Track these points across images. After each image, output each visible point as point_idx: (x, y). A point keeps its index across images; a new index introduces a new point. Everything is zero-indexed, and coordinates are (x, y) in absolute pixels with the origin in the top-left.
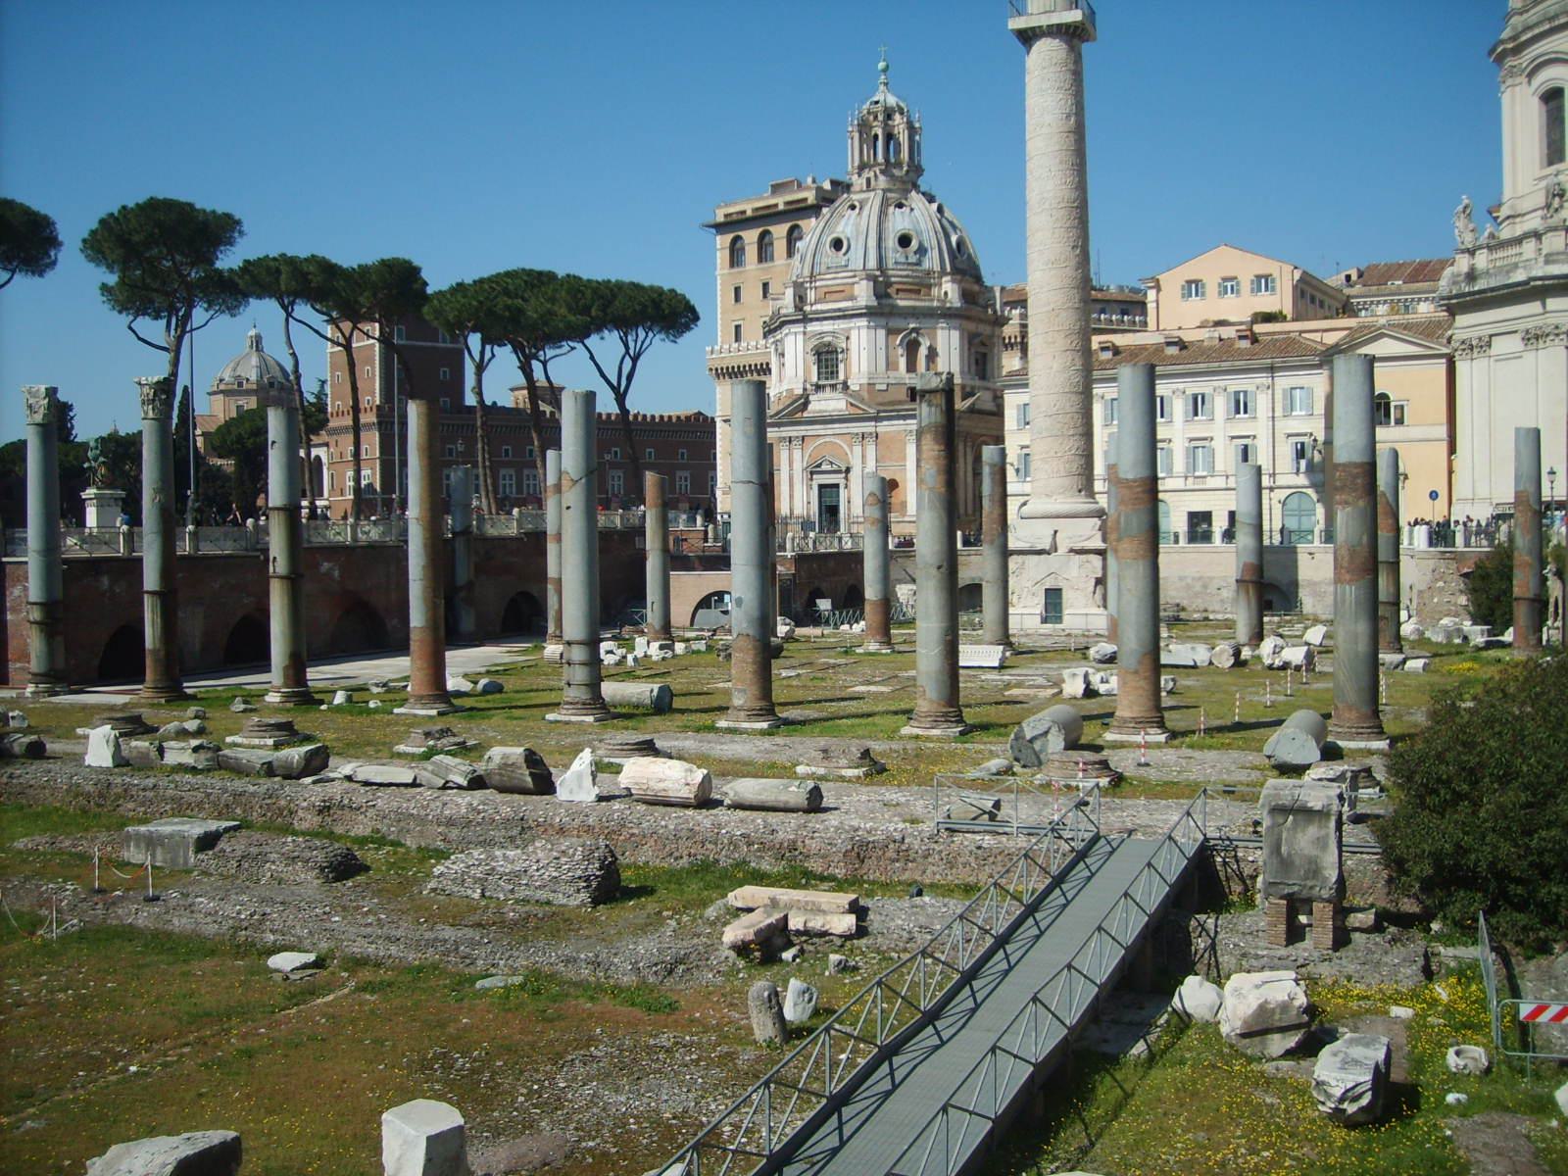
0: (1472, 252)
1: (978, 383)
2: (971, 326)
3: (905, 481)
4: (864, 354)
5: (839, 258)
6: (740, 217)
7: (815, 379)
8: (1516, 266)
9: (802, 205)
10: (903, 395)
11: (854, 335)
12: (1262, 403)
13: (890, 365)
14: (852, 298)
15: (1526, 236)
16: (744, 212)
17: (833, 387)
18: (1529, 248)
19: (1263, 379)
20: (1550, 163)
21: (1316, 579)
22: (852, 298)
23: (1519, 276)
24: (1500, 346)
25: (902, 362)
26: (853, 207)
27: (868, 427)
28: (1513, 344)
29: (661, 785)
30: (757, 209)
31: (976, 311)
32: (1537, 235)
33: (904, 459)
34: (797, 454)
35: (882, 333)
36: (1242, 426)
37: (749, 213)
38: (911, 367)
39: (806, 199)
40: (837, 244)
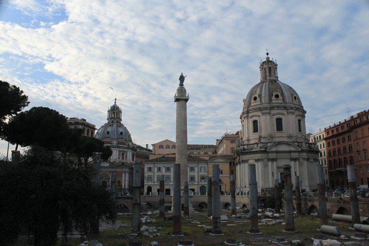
12: (196, 169)
13: (119, 158)
17: (107, 162)
18: (256, 146)
19: (196, 165)
20: (254, 132)
23: (254, 150)
27: (114, 170)
32: (257, 144)
33: (122, 177)
35: (117, 153)
36: (192, 174)
38: (123, 158)
40: (108, 133)
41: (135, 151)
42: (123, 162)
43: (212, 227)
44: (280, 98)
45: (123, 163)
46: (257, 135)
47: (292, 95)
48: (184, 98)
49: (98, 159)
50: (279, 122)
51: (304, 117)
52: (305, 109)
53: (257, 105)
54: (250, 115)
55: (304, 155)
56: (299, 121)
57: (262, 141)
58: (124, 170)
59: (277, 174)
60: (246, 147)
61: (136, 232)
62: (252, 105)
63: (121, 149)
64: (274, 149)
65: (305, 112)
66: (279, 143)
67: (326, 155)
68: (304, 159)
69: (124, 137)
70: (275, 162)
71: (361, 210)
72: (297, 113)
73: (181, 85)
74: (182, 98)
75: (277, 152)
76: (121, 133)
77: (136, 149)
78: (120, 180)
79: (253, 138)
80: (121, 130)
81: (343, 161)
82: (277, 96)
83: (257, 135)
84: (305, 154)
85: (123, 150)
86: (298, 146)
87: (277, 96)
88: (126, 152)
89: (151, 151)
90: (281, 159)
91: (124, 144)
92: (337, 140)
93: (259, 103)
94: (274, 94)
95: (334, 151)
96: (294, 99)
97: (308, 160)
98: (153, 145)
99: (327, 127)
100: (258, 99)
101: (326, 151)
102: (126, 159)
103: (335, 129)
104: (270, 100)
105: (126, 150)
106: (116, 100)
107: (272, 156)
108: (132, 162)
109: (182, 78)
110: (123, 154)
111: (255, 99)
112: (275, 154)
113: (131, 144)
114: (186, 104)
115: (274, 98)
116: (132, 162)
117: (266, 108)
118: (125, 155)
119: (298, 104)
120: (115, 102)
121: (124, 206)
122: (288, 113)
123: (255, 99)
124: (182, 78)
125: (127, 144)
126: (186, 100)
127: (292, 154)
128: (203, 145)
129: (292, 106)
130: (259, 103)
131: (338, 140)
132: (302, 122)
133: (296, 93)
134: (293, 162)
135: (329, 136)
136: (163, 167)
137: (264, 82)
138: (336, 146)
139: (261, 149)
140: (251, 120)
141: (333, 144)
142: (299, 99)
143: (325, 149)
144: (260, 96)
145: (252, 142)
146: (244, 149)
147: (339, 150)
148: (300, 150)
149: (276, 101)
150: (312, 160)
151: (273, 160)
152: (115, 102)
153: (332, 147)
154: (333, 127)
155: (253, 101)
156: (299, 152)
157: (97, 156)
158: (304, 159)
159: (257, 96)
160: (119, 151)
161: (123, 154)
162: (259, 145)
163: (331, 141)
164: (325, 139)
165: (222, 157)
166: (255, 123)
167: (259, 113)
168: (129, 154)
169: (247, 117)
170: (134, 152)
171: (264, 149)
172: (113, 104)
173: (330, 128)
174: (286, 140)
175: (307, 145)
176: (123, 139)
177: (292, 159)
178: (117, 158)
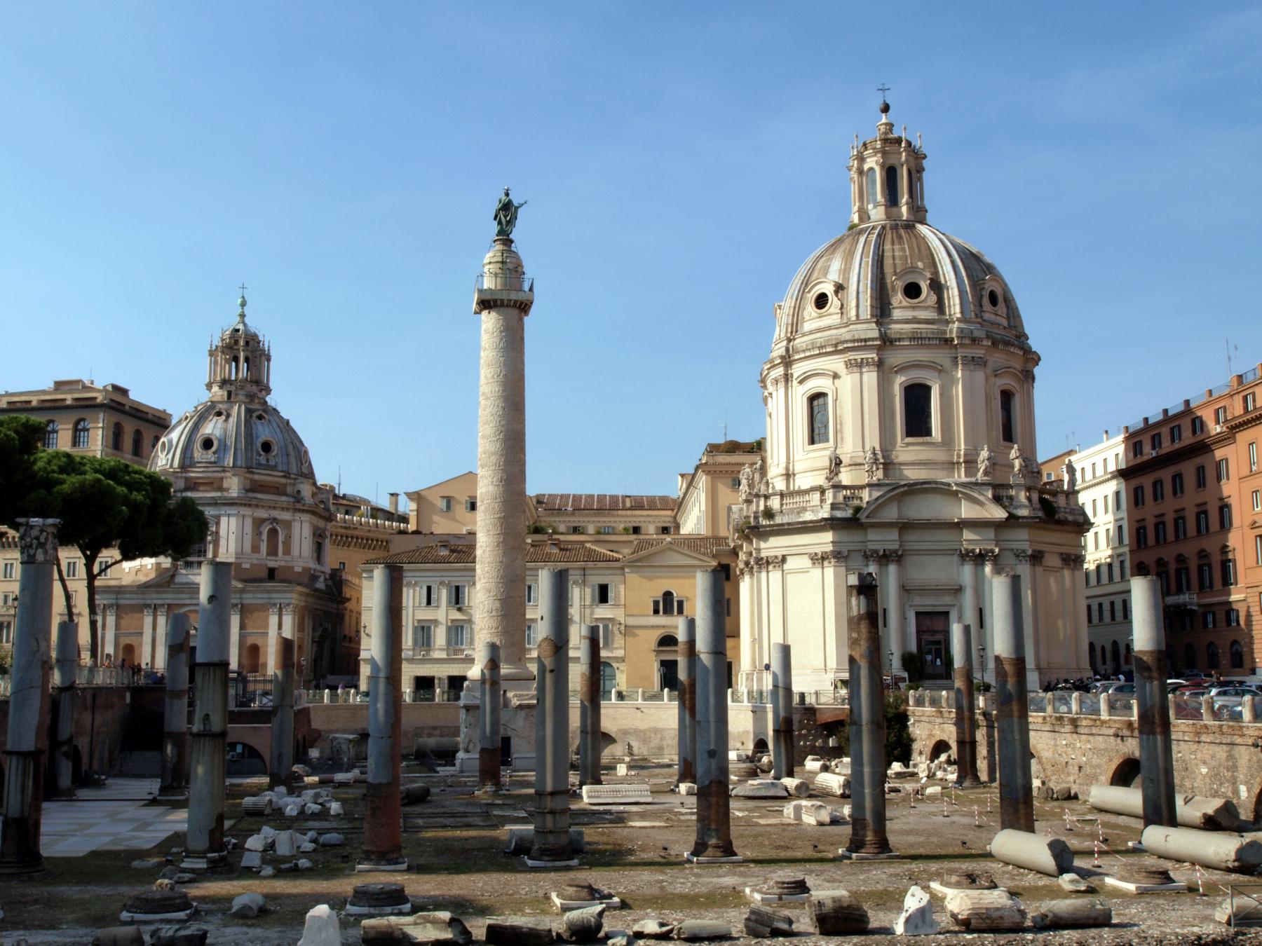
0: (766, 497)
1: (318, 567)
2: (315, 520)
3: (267, 646)
4: (232, 538)
5: (210, 456)
6: (24, 406)
8: (804, 509)
9: (58, 404)
10: (264, 574)
11: (224, 520)
13: (255, 549)
14: (220, 489)
15: (813, 489)
16: (30, 402)
18: (816, 496)
21: (642, 728)
22: (220, 489)
23: (808, 516)
24: (791, 564)
25: (264, 547)
26: (219, 414)
28: (805, 562)
30: (43, 401)
31: (299, 506)
33: (267, 626)
35: (249, 522)
37: (34, 403)
38: (273, 551)
39: (95, 398)
40: (208, 444)
41: (330, 518)
42: (272, 564)
43: (532, 827)
45: (271, 574)
46: (821, 454)
47: (976, 284)
48: (514, 296)
49: (41, 545)
50: (917, 399)
51: (1029, 377)
52: (1034, 343)
53: (830, 328)
54: (798, 370)
55: (1022, 539)
56: (1007, 396)
57: (846, 478)
58: (278, 598)
59: (903, 618)
60: (775, 503)
61: (201, 854)
62: (807, 327)
63: (262, 514)
64: (891, 514)
65: (1032, 358)
66: (916, 489)
67: (1126, 541)
68: (1019, 555)
69: (272, 459)
70: (892, 568)
71: (1204, 770)
72: (997, 359)
73: (505, 238)
74: (505, 296)
75: (905, 527)
76: (267, 447)
77: (328, 506)
78: (259, 642)
79: (808, 465)
80: (264, 432)
81: (1193, 564)
82: (912, 291)
83: (821, 454)
84: (1023, 534)
86: (997, 499)
88: (288, 525)
89: (404, 519)
90: (920, 552)
91: (278, 490)
92: (1155, 484)
93: (835, 319)
94: (900, 285)
95: (1160, 525)
96: (986, 301)
97: (1036, 558)
98: (417, 497)
99: (1136, 422)
100: (834, 303)
101: (1125, 524)
102: (287, 551)
103: (1165, 431)
104: (882, 309)
105: (286, 516)
106: (243, 304)
107: (886, 540)
108: (312, 565)
109: (507, 212)
110: (273, 532)
111: (821, 301)
112: (893, 535)
113: (306, 490)
114: (521, 320)
115: (898, 299)
116: (312, 565)
117: (863, 345)
118: (281, 538)
120: (242, 316)
121: (245, 745)
123: (821, 301)
124: (507, 212)
125: (289, 490)
126: (524, 307)
127: (967, 535)
128: (625, 497)
129: (977, 334)
130: (835, 319)
131: (1177, 479)
132: (1017, 402)
133: (997, 277)
134: (968, 570)
135: (1139, 460)
136: (442, 583)
137: (861, 232)
138: (1169, 505)
139: (839, 514)
140: (800, 394)
141: (1157, 495)
142: (1009, 302)
143: (1124, 514)
144: (839, 288)
145: (802, 482)
146: (769, 514)
147: (1180, 519)
148: (999, 513)
149: (909, 314)
150: (1052, 560)
151: (885, 558)
152: (242, 316)
153: (1150, 510)
154: (1158, 424)
155: (810, 309)
156: (998, 525)
157: (35, 532)
158: (1019, 555)
159: (828, 289)
160: (258, 523)
161: (273, 532)
162: (829, 495)
163: (1147, 481)
164: (1122, 474)
165: (694, 543)
166: (816, 399)
167: (836, 363)
168: (302, 531)
169: (787, 378)
170: (321, 523)
171: (848, 513)
172: (234, 322)
173: (1148, 426)
175: (1035, 496)
176: (274, 468)
177: (965, 556)
178: (248, 546)
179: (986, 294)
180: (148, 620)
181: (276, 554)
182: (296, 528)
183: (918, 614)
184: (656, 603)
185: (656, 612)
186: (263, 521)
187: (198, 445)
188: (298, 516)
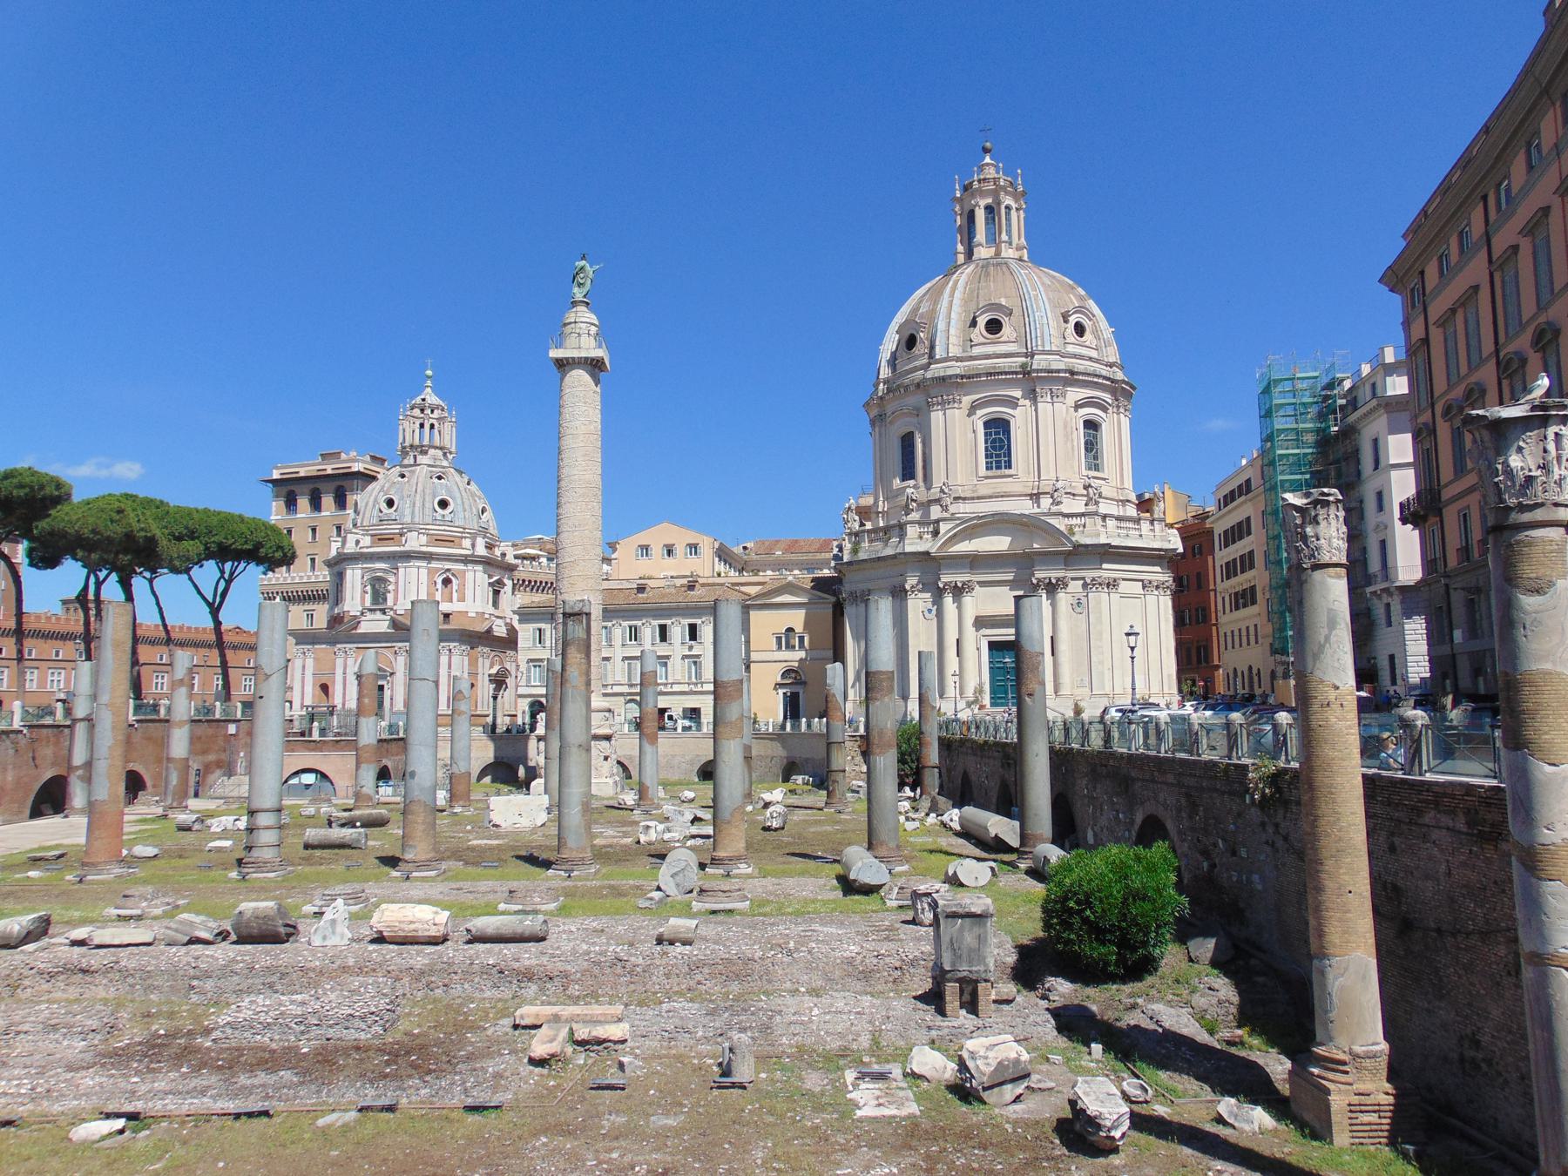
7: (368, 603)
11: (401, 571)
29: (412, 927)
34: (350, 661)
35: (424, 572)
44: (1007, 331)
45: (447, 616)
56: (1091, 425)
85: (448, 565)
87: (994, 326)
91: (449, 541)
97: (1112, 584)
110: (447, 582)
118: (455, 587)
119: (1094, 354)
122: (1032, 395)
149: (990, 349)
160: (431, 572)
161: (447, 582)
174: (1025, 507)
179: (1071, 325)
180: (339, 662)
181: (451, 601)
182: (469, 575)
183: (990, 644)
184: (779, 639)
185: (780, 648)
186: (437, 570)
187: (384, 506)
188: (470, 567)
